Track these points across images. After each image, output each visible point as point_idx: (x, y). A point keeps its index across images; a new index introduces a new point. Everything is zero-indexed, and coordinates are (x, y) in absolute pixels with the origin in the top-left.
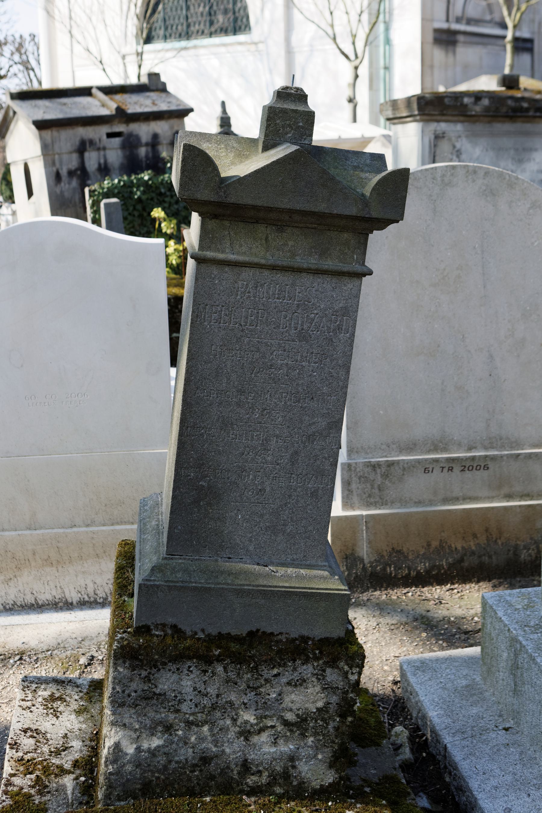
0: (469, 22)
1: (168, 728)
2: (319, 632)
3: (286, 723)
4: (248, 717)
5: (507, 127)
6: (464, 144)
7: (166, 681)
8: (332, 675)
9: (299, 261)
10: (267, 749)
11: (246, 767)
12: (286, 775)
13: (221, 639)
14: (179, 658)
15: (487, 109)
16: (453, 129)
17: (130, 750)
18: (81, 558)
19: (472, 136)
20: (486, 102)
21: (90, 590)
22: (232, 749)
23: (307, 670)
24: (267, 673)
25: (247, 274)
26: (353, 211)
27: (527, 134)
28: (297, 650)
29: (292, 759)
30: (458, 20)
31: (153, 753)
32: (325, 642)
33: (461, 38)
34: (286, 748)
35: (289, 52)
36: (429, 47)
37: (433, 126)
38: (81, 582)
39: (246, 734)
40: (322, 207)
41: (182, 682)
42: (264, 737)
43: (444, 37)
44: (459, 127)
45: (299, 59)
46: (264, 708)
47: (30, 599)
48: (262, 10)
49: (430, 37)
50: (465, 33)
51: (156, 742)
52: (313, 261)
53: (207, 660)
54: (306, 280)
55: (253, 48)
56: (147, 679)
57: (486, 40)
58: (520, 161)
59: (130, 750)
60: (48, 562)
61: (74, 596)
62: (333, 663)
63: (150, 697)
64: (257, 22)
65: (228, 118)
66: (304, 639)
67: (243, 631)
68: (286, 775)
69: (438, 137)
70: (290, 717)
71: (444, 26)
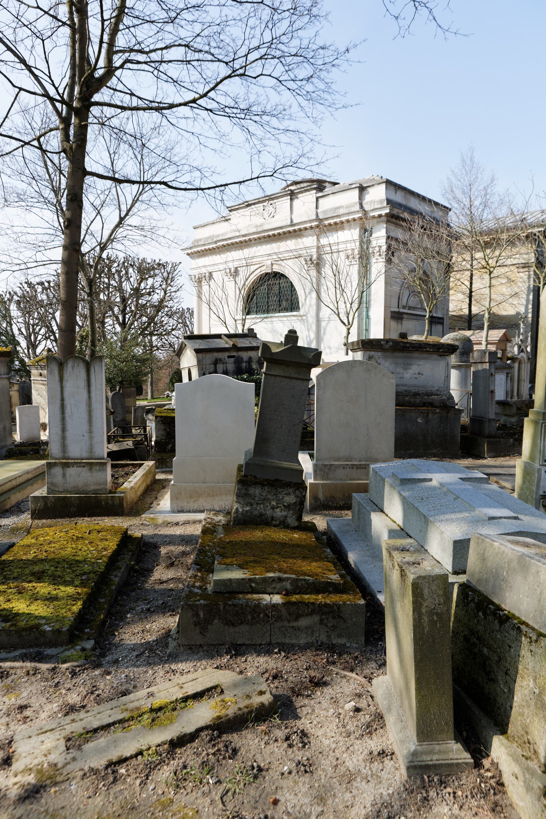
0: (410, 308)
1: (251, 505)
2: (294, 481)
3: (284, 506)
4: (274, 503)
5: (400, 354)
6: (381, 361)
7: (251, 491)
8: (298, 493)
9: (292, 376)
10: (279, 513)
11: (273, 518)
13: (267, 480)
14: (256, 484)
15: (391, 346)
16: (377, 354)
17: (241, 510)
21: (223, 507)
22: (269, 512)
23: (291, 490)
25: (278, 378)
28: (288, 485)
29: (286, 517)
30: (404, 307)
31: (247, 511)
32: (296, 484)
33: (405, 316)
34: (284, 513)
35: (318, 321)
36: (388, 320)
37: (368, 353)
38: (220, 503)
39: (273, 508)
40: (298, 360)
41: (256, 491)
42: (278, 510)
43: (397, 315)
44: (379, 353)
45: (323, 324)
46: (279, 501)
48: (306, 300)
49: (389, 316)
50: (407, 314)
51: (248, 508)
52: (296, 376)
54: (294, 381)
55: (300, 318)
56: (246, 489)
57: (418, 318)
58: (406, 369)
59: (241, 510)
60: (209, 495)
62: (298, 489)
63: (247, 495)
64: (302, 306)
66: (290, 482)
67: (273, 479)
70: (285, 504)
71: (397, 310)
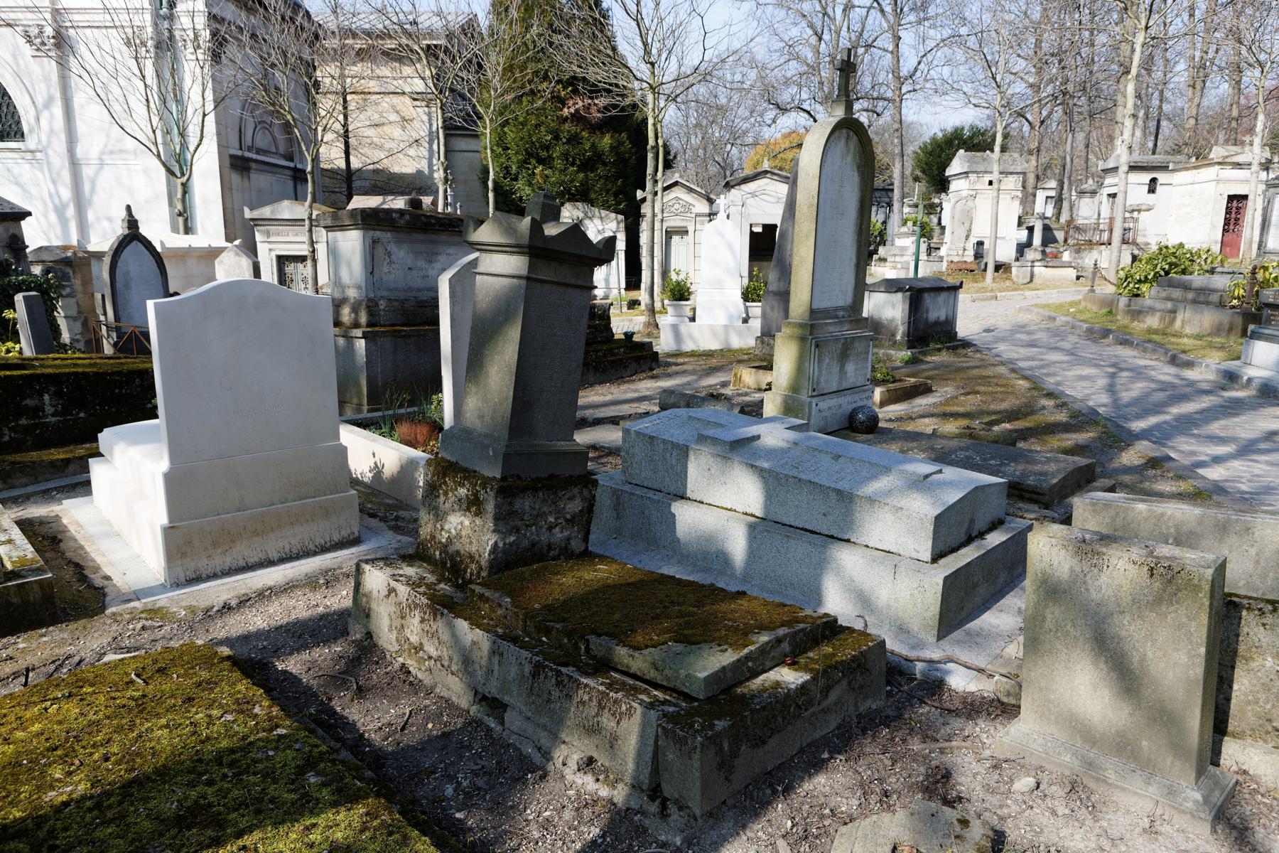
0: (259, 151)
1: (518, 530)
2: (577, 472)
3: (567, 520)
4: (551, 519)
5: (421, 236)
6: (392, 248)
7: (518, 504)
8: (586, 492)
9: (568, 281)
10: (559, 535)
11: (550, 546)
12: (566, 548)
13: (538, 479)
14: (524, 490)
15: (408, 223)
16: (385, 236)
17: (501, 545)
18: (280, 526)
19: (399, 242)
20: (407, 217)
21: (287, 549)
22: (545, 537)
23: (576, 490)
24: (561, 494)
25: (547, 287)
26: (595, 256)
27: (433, 242)
28: (570, 482)
29: (569, 539)
30: (250, 149)
31: (511, 544)
32: (580, 477)
33: (253, 165)
34: (566, 533)
35: (74, 164)
36: (227, 170)
37: (371, 233)
38: (281, 545)
39: (550, 528)
40: (584, 253)
41: (525, 504)
42: (557, 530)
43: (239, 163)
44: (389, 235)
45: (87, 172)
46: (559, 513)
47: (242, 563)
48: (38, 119)
49: (227, 162)
50: (256, 161)
51: (512, 539)
52: (573, 281)
53: (536, 490)
54: (570, 290)
55: (29, 156)
56: (510, 504)
57: (274, 169)
58: (431, 262)
59: (501, 545)
60: (255, 533)
61: (275, 556)
62: (586, 486)
63: (512, 514)
64: (31, 131)
65: (136, 221)
66: (571, 476)
67: (546, 475)
68: (566, 548)
69: (375, 242)
70: (568, 516)
71: (239, 153)
